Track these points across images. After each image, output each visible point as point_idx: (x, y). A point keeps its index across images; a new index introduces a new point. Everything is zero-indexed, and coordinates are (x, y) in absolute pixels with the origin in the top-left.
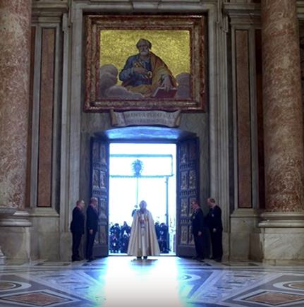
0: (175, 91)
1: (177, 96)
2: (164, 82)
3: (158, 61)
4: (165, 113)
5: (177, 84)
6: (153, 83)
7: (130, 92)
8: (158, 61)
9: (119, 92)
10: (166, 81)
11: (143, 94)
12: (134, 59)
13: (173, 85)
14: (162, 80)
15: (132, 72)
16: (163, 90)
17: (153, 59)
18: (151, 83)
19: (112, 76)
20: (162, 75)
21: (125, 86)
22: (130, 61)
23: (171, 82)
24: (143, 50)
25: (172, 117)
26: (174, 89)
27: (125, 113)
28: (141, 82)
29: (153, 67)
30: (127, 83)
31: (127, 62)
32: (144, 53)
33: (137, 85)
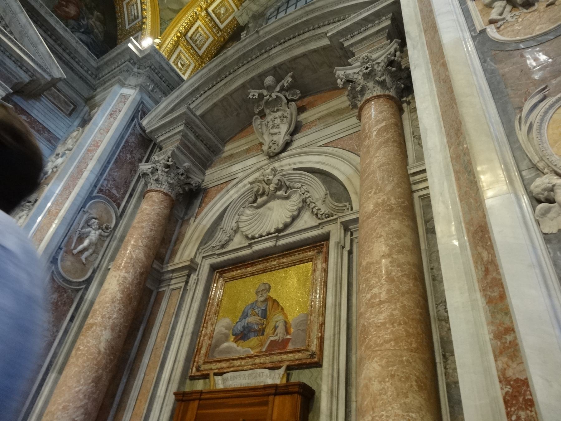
0: (289, 340)
1: (290, 347)
2: (278, 330)
3: (275, 305)
4: (267, 371)
5: (292, 330)
6: (265, 333)
7: (240, 348)
8: (275, 305)
9: (228, 350)
10: (281, 329)
11: (252, 349)
12: (250, 308)
13: (287, 331)
14: (275, 328)
15: (246, 322)
16: (276, 340)
17: (270, 303)
18: (263, 334)
19: (227, 331)
20: (277, 322)
21: (235, 342)
22: (246, 310)
23: (286, 327)
24: (262, 296)
25: (277, 376)
26: (288, 337)
27: (225, 376)
28: (253, 333)
29: (268, 313)
30: (239, 337)
31: (244, 312)
32: (262, 299)
33: (248, 339)
